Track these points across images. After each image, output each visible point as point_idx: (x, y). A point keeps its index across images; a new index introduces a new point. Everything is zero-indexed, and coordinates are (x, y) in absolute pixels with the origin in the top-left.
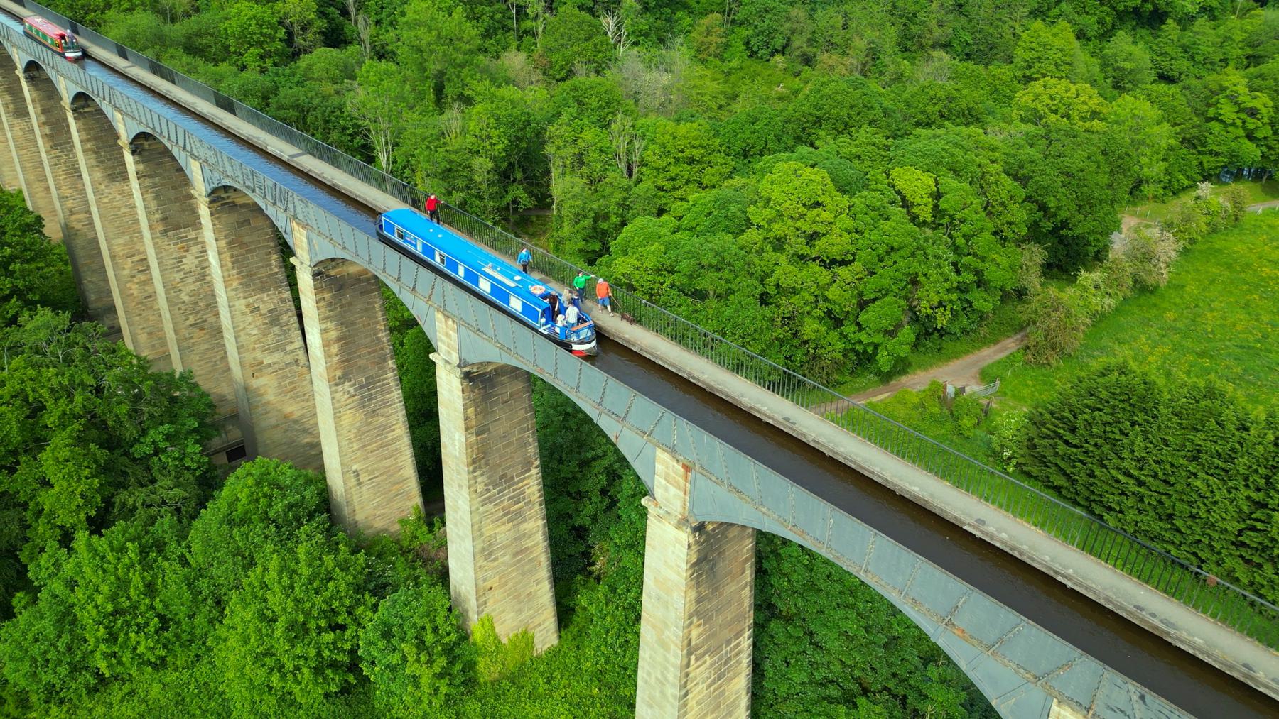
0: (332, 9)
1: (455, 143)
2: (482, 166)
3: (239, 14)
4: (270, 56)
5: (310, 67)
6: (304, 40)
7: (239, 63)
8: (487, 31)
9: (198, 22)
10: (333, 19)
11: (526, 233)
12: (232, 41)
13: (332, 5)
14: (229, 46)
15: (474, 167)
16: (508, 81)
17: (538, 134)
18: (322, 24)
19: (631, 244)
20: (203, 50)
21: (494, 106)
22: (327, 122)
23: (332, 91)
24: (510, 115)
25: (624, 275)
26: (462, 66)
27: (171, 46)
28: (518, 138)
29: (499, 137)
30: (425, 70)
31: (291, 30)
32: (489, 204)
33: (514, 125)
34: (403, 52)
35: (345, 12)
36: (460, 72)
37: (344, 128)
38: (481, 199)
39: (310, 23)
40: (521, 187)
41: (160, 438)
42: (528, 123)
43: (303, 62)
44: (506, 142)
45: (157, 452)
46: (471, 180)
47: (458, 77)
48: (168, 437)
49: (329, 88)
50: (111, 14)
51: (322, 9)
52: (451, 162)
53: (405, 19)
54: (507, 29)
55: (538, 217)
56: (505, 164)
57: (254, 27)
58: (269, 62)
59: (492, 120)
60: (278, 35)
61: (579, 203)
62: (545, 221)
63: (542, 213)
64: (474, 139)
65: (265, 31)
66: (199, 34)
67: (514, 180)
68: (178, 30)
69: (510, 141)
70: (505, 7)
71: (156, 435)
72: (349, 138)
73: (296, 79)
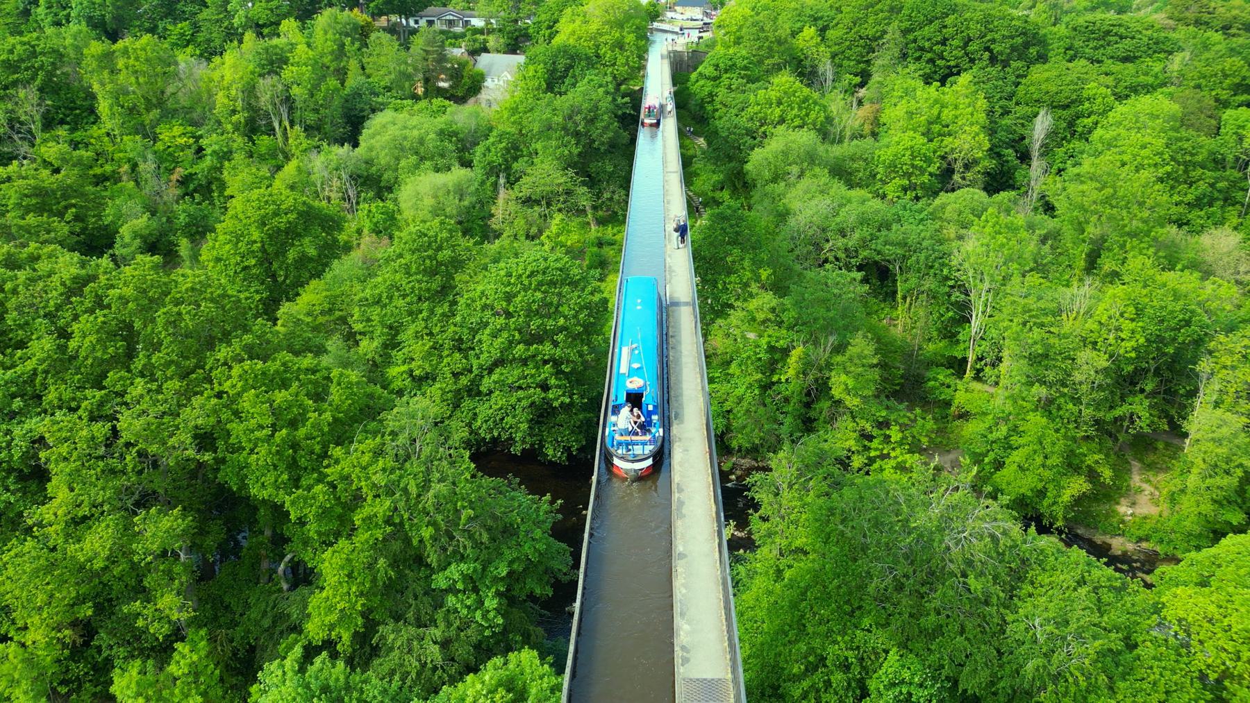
0: (1010, 151)
1: (1067, 326)
2: (1089, 365)
3: (898, 143)
4: (915, 189)
5: (943, 207)
6: (963, 178)
7: (881, 191)
8: (1198, 199)
9: (857, 146)
10: (1007, 161)
11: (1141, 461)
12: (881, 169)
13: (1013, 147)
14: (878, 173)
15: (1079, 361)
16: (1193, 266)
17: (1198, 342)
18: (989, 164)
19: (1218, 573)
20: (850, 174)
21: (1144, 292)
22: (931, 267)
23: (953, 236)
24: (1162, 308)
25: (1180, 621)
26: (1133, 235)
27: (819, 165)
28: (1160, 339)
29: (1133, 332)
30: (1083, 231)
31: (953, 165)
32: (1088, 412)
33: (1162, 321)
34: (1061, 205)
35: (1025, 157)
36: (1125, 242)
37: (947, 278)
38: (1077, 401)
39: (976, 162)
40: (1147, 403)
41: (456, 576)
42: (1188, 323)
43: (943, 198)
44: (1142, 340)
45: (451, 590)
46: (1069, 375)
47: (1122, 246)
48: (467, 578)
49: (951, 231)
50: (781, 128)
51: (998, 150)
52: (1048, 347)
53: (1076, 170)
54: (1228, 200)
55: (1167, 445)
56: (1130, 368)
57: (906, 159)
58: (910, 194)
59: (1131, 309)
60: (929, 169)
61: (1223, 451)
62: (1175, 451)
63: (1176, 441)
64: (1095, 327)
65: (916, 163)
66: (853, 159)
67: (1142, 391)
68: (837, 151)
69: (1147, 340)
70: (1240, 174)
71: (455, 571)
72: (947, 289)
73: (921, 216)
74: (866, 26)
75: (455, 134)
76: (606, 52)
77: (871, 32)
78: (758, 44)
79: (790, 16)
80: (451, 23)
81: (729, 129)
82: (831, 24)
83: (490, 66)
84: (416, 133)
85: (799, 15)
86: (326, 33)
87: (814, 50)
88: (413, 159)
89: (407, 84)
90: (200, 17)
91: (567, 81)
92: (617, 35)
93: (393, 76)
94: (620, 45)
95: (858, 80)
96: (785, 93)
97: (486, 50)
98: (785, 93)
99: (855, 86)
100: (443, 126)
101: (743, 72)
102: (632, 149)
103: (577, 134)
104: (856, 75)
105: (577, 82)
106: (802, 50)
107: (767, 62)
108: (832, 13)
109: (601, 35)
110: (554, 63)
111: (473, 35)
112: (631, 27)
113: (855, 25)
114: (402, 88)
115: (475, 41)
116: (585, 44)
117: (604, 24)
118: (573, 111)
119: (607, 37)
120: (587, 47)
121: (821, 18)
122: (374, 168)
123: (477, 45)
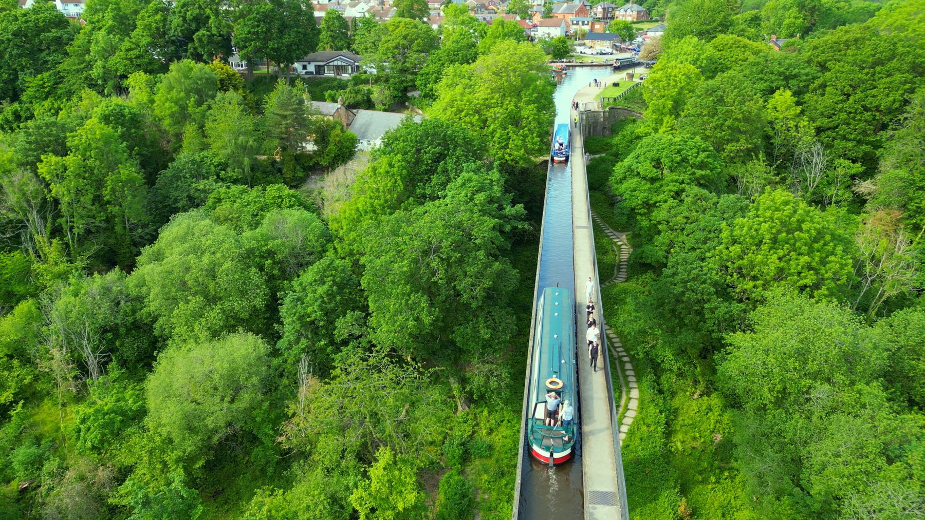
74: (874, 92)
75: (271, 254)
76: (494, 131)
77: (885, 103)
78: (715, 121)
79: (747, 72)
80: (339, 69)
81: (685, 282)
82: (812, 87)
83: (367, 126)
84: (206, 259)
85: (761, 72)
86: (171, 88)
87: (792, 124)
88: (196, 301)
89: (246, 161)
90: (60, 67)
91: (434, 179)
92: (511, 107)
93: (229, 151)
94: (516, 121)
95: (858, 168)
96: (783, 224)
97: (369, 104)
98: (783, 224)
99: (853, 177)
100: (253, 244)
101: (699, 173)
102: (529, 274)
103: (431, 291)
104: (854, 161)
105: (449, 181)
106: (771, 123)
107: (728, 147)
108: (813, 70)
109: (489, 107)
110: (418, 151)
111: (356, 84)
112: (531, 95)
113: (854, 88)
114: (240, 165)
115: (357, 92)
116: (467, 119)
117: (493, 91)
118: (430, 248)
119: (497, 109)
120: (468, 127)
121: (795, 76)
122: (145, 310)
123: (360, 97)
